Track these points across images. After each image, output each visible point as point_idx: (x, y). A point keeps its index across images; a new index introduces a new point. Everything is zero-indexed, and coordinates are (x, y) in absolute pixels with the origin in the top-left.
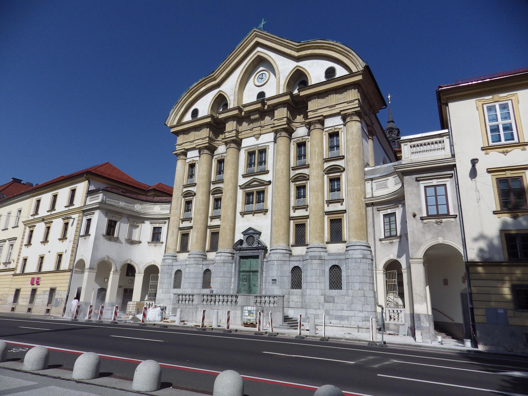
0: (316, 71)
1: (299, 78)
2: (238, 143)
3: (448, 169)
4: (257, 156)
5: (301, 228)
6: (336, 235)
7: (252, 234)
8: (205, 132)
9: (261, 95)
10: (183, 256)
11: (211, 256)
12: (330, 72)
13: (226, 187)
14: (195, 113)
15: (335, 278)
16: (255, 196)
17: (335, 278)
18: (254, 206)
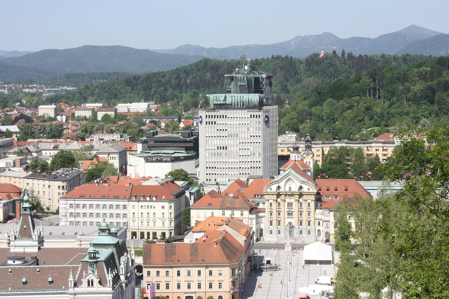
0: (305, 189)
1: (301, 188)
2: (285, 201)
3: (329, 221)
4: (290, 204)
5: (301, 222)
6: (309, 224)
7: (290, 223)
8: (275, 196)
9: (290, 187)
10: (271, 227)
11: (279, 227)
12: (309, 189)
13: (282, 210)
14: (271, 189)
15: (309, 232)
16: (290, 214)
17: (309, 232)
18: (290, 216)
